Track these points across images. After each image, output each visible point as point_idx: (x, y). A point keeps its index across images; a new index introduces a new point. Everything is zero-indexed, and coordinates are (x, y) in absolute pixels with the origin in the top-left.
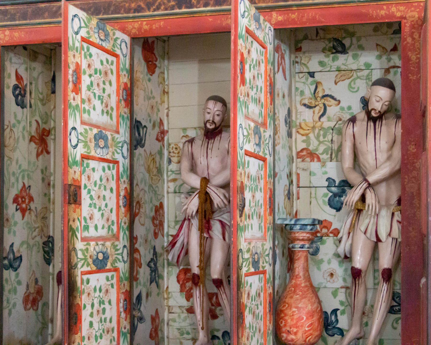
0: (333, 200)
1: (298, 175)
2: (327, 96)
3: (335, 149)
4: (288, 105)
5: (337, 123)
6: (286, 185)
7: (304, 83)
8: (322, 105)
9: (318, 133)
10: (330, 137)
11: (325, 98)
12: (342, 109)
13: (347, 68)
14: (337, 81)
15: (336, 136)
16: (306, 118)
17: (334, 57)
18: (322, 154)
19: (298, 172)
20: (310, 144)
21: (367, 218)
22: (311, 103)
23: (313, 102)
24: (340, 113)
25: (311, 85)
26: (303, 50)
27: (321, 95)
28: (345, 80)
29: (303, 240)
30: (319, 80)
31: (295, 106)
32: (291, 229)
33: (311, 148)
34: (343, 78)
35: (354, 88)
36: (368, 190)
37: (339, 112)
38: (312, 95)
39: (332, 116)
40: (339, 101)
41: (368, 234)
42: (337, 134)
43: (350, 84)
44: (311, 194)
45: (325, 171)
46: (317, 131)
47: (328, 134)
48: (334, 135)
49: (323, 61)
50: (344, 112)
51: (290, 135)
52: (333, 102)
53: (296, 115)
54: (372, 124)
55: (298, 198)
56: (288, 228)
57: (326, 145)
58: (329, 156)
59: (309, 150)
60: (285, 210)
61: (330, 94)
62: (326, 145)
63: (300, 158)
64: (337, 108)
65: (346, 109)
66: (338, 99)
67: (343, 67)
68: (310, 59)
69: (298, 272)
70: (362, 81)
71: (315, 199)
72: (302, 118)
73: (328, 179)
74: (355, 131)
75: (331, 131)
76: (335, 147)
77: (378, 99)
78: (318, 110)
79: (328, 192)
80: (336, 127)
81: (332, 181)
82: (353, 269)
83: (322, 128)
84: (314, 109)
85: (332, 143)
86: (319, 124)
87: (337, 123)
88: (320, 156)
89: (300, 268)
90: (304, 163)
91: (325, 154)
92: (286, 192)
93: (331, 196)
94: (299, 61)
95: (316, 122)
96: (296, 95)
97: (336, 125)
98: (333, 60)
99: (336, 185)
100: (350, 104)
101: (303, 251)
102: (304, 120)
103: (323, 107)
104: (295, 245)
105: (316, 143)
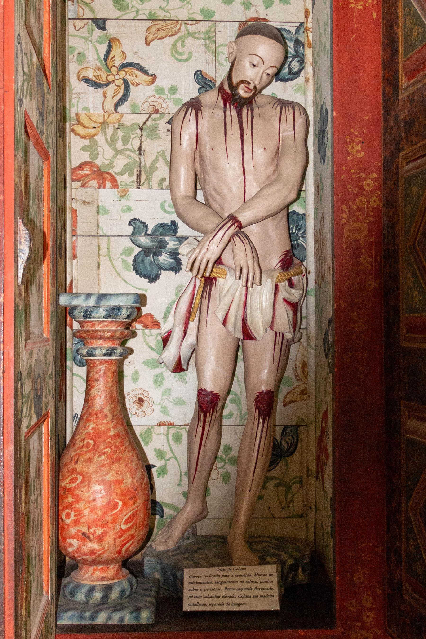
0: (143, 261)
1: (74, 212)
2: (131, 65)
3: (145, 165)
5: (150, 116)
8: (120, 83)
10: (136, 144)
12: (160, 91)
13: (168, 15)
14: (150, 38)
16: (90, 106)
18: (121, 174)
19: (74, 206)
20: (98, 154)
22: (99, 77)
23: (104, 76)
24: (155, 99)
25: (100, 43)
27: (118, 62)
28: (165, 37)
30: (115, 36)
33: (99, 162)
34: (161, 34)
37: (154, 96)
38: (100, 61)
39: (140, 104)
40: (154, 77)
43: (174, 45)
44: (99, 248)
45: (127, 206)
46: (110, 131)
47: (133, 136)
48: (144, 138)
50: (163, 96)
52: (142, 77)
54: (234, 113)
55: (74, 257)
57: (128, 157)
58: (134, 178)
59: (96, 165)
62: (128, 157)
63: (78, 180)
64: (150, 90)
65: (167, 92)
66: (151, 72)
67: (161, 14)
71: (107, 258)
72: (82, 105)
73: (133, 222)
75: (139, 131)
77: (256, 60)
79: (133, 246)
80: (148, 123)
81: (141, 225)
83: (120, 126)
84: (105, 89)
85: (140, 154)
86: (115, 117)
87: (150, 116)
88: (116, 177)
90: (85, 190)
93: (138, 254)
97: (147, 120)
99: (149, 232)
102: (85, 108)
105: (109, 152)
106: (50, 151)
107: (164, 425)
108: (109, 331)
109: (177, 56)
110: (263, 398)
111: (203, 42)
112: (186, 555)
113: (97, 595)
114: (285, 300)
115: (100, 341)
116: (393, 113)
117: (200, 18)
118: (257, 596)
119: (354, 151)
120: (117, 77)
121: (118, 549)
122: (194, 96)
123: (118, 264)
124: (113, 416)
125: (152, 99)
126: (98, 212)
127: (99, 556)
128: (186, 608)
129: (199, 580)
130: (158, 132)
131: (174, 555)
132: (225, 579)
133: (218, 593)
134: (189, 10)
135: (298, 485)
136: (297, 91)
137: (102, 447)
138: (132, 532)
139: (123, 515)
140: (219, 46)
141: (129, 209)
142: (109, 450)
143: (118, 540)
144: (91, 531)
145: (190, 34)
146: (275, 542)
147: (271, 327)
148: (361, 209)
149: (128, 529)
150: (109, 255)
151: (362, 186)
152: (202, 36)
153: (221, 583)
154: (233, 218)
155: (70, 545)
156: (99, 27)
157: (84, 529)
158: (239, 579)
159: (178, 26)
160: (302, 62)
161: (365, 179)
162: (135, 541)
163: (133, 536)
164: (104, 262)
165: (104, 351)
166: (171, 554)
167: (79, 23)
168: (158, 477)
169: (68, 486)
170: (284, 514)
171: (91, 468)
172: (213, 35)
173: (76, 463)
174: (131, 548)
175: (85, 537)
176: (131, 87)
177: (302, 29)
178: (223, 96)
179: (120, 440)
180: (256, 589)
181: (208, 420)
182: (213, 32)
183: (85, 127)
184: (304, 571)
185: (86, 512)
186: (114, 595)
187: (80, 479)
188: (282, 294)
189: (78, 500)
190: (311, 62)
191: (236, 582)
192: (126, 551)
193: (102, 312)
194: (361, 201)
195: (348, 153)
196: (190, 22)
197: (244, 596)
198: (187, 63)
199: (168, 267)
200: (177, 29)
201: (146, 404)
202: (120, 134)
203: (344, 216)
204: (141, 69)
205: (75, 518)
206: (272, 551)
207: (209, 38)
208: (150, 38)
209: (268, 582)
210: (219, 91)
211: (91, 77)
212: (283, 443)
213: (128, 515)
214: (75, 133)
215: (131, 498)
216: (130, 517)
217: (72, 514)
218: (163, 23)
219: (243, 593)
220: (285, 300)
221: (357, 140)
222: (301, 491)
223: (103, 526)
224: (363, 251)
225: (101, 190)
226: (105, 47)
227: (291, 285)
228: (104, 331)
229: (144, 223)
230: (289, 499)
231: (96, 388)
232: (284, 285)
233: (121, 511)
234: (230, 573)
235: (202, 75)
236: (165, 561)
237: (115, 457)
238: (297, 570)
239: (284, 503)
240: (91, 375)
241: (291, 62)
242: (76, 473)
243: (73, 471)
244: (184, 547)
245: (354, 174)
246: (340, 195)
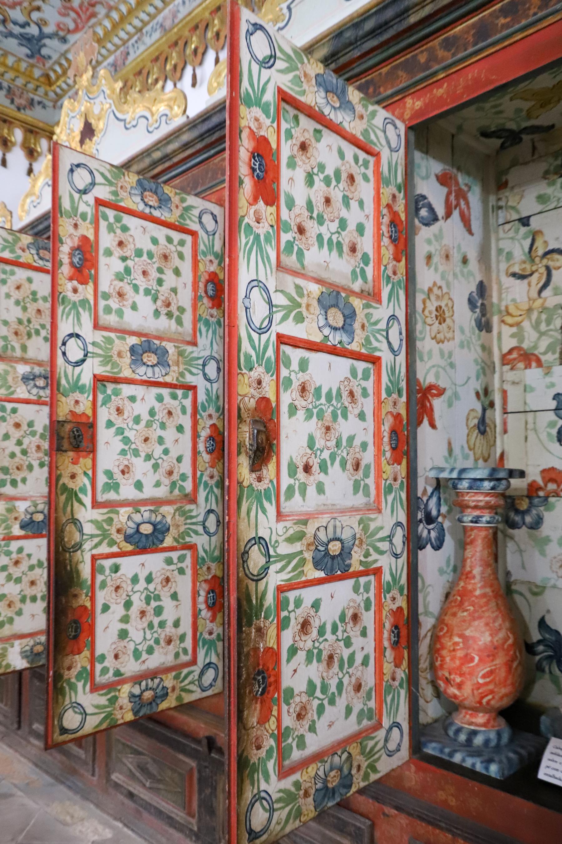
1: (504, 393)
7: (512, 238)
8: (543, 270)
18: (545, 353)
22: (524, 270)
23: (528, 266)
25: (525, 238)
26: (510, 185)
33: (525, 346)
44: (526, 423)
46: (535, 316)
53: (500, 293)
55: (505, 431)
57: (551, 336)
60: (471, 453)
62: (551, 336)
63: (507, 364)
68: (522, 197)
71: (533, 432)
78: (536, 280)
83: (544, 309)
86: (539, 302)
90: (514, 372)
91: (550, 353)
95: (534, 301)
102: (514, 300)
123: (543, 436)
124: (482, 577)
137: (466, 604)
142: (472, 608)
150: (535, 430)
162: (497, 697)
163: (492, 692)
164: (532, 436)
167: (507, 227)
179: (485, 600)
213: (485, 671)
216: (487, 672)
225: (528, 371)
226: (529, 241)
237: (476, 615)
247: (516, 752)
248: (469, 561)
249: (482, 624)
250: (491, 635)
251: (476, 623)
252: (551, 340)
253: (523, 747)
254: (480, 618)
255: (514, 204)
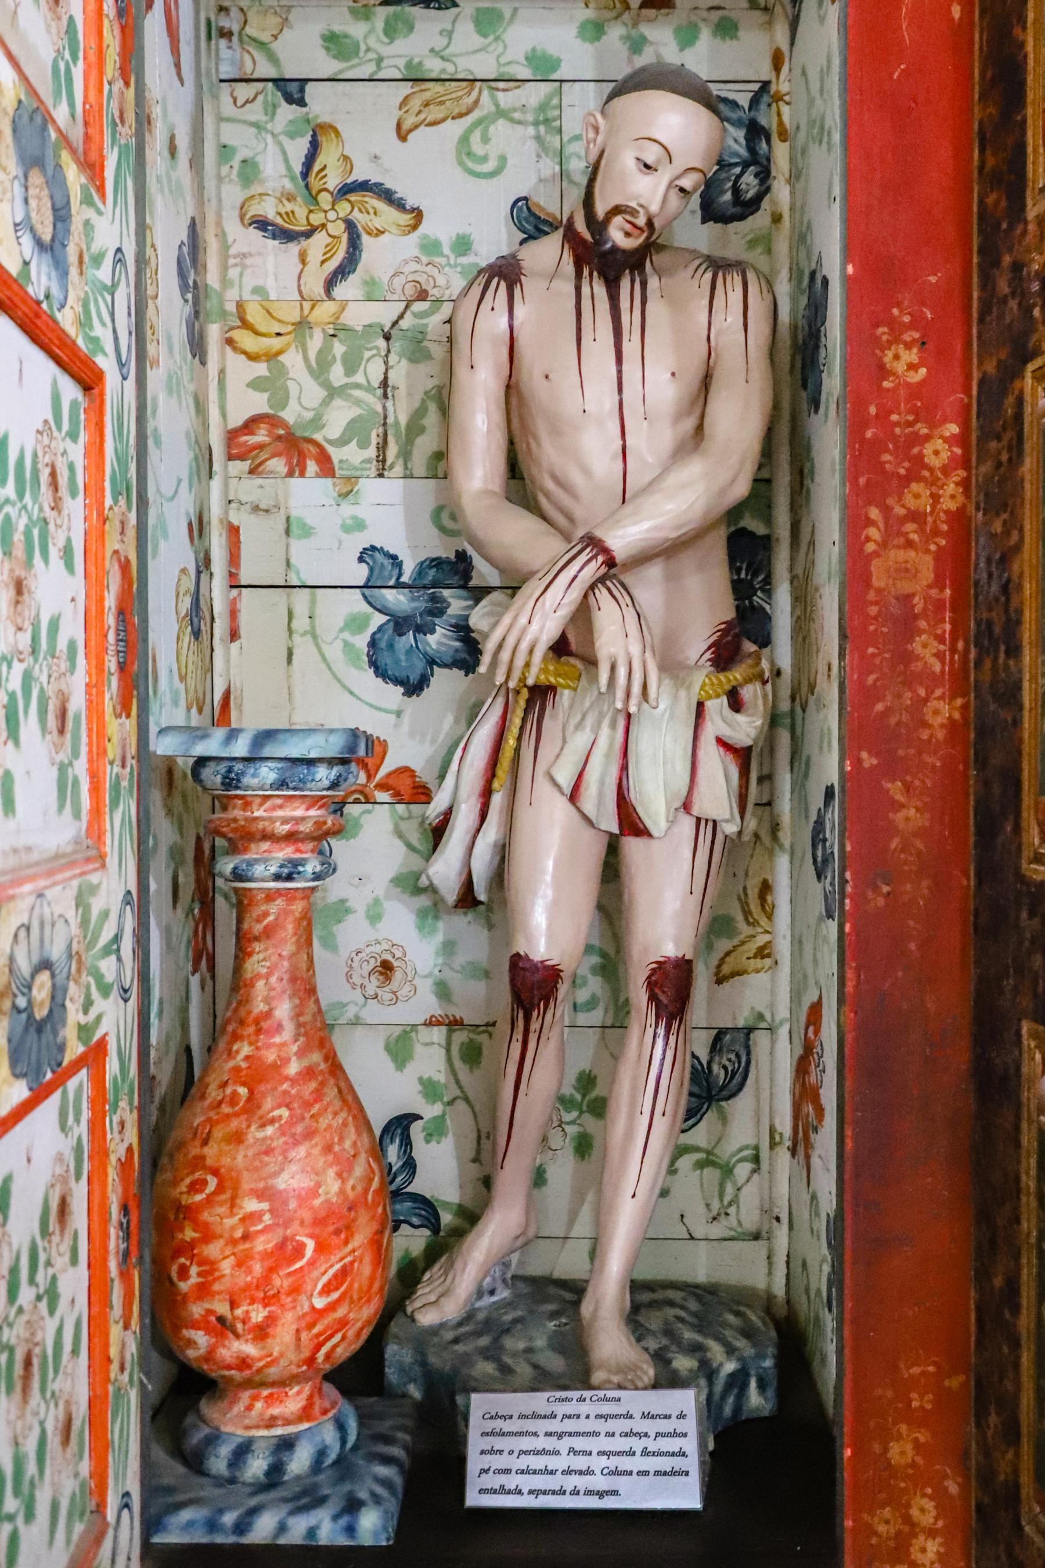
0: (391, 646)
1: (233, 531)
2: (363, 186)
3: (397, 423)
4: (191, 212)
5: (407, 307)
6: (184, 571)
7: (256, 125)
8: (338, 229)
9: (320, 352)
10: (375, 371)
11: (353, 197)
12: (431, 247)
13: (450, 68)
14: (409, 122)
15: (404, 362)
16: (271, 285)
17: (396, 17)
18: (342, 442)
19: (234, 519)
20: (287, 397)
21: (579, 726)
22: (290, 215)
23: (301, 212)
24: (418, 267)
25: (292, 136)
27: (333, 181)
29: (291, 837)
31: (219, 223)
32: (230, 781)
33: (289, 415)
34: (435, 112)
35: (485, 159)
36: (602, 594)
37: (417, 260)
38: (293, 178)
39: (385, 279)
40: (418, 214)
41: (589, 802)
42: (412, 360)
43: (464, 139)
45: (355, 518)
46: (315, 342)
47: (367, 354)
48: (393, 359)
49: (346, 36)
51: (197, 347)
52: (388, 215)
53: (224, 268)
54: (601, 290)
55: (234, 635)
56: (212, 776)
57: (358, 402)
58: (372, 452)
59: (283, 423)
60: (182, 687)
61: (374, 179)
62: (358, 402)
63: (241, 457)
65: (446, 250)
66: (410, 203)
67: (434, 66)
69: (267, 1000)
70: (520, 128)
71: (308, 638)
72: (249, 282)
74: (516, 323)
75: (382, 343)
76: (401, 412)
80: (404, 324)
81: (387, 562)
82: (518, 964)
83: (338, 331)
84: (304, 243)
87: (407, 307)
88: (330, 449)
89: (273, 980)
92: (186, 603)
93: (380, 629)
94: (235, 28)
96: (220, 179)
97: (401, 317)
98: (390, 32)
99: (405, 579)
100: (468, 230)
101: (289, 895)
102: (258, 290)
103: (345, 238)
104: (250, 863)
105: (314, 394)
106: (106, 363)
107: (439, 1023)
108: (285, 821)
109: (470, 164)
110: (666, 975)
111: (531, 130)
112: (484, 1341)
113: (257, 1466)
114: (720, 741)
115: (265, 846)
116: (1007, 260)
117: (525, 73)
118: (645, 1473)
119: (900, 367)
120: (332, 215)
121: (306, 1353)
122: (505, 251)
123: (335, 652)
124: (299, 1025)
125: (414, 266)
126: (287, 532)
127: (259, 1371)
128: (473, 1499)
129: (507, 1426)
130: (425, 343)
131: (456, 1341)
132: (570, 1426)
133: (552, 1462)
134: (498, 57)
135: (748, 1166)
136: (752, 244)
137: (268, 1103)
138: (341, 1312)
139: (316, 1274)
140: (570, 141)
141: (359, 525)
142: (284, 1112)
143: (304, 1336)
144: (239, 1312)
145: (501, 113)
146: (693, 1305)
147: (687, 806)
148: (915, 516)
149: (331, 1307)
151: (921, 457)
152: (530, 118)
153: (560, 1436)
154: (593, 542)
155: (191, 1343)
156: (290, 99)
157: (222, 1308)
158: (601, 1426)
159: (475, 94)
160: (765, 175)
161: (928, 438)
162: (351, 1333)
163: (343, 1323)
164: (303, 647)
165: (273, 869)
166: (450, 1335)
167: (244, 91)
168: (428, 1142)
169: (186, 1200)
170: (716, 1230)
171: (240, 1158)
172: (557, 113)
173: (205, 1142)
174: (339, 1350)
175: (223, 1327)
176: (365, 239)
177: (766, 99)
178: (574, 249)
179: (313, 1085)
180: (645, 1453)
181: (535, 1026)
182: (554, 108)
183: (257, 333)
184: (762, 1386)
185: (226, 1266)
186: (299, 1462)
187: (212, 1183)
188: (714, 725)
189: (208, 1236)
190: (787, 175)
191: (596, 1434)
192: (328, 1356)
193: (267, 773)
194: (917, 496)
195: (883, 371)
196: (501, 85)
197: (616, 1473)
198: (494, 180)
199: (448, 660)
200: (470, 100)
201: (398, 975)
202: (339, 348)
203: (873, 532)
204: (388, 196)
205: (201, 1280)
206: (689, 1335)
207: (546, 121)
208: (409, 122)
209: (675, 1434)
210: (565, 236)
211: (271, 215)
212: (715, 1068)
213: (331, 1272)
214: (235, 349)
215: (337, 1232)
216: (335, 1276)
217: (194, 1270)
218: (437, 88)
219: (614, 1462)
220: (720, 741)
221: (907, 337)
222: (756, 1176)
223: (266, 1302)
224: (923, 624)
225: (296, 482)
227: (736, 703)
228: (272, 820)
229: (394, 557)
230: (727, 1199)
231: (255, 958)
232: (716, 707)
233: (312, 1263)
234: (584, 1409)
235: (529, 209)
236: (433, 1360)
237: (299, 1129)
238: (744, 1387)
239: (716, 1205)
240: (246, 926)
241: (739, 177)
242: (204, 1167)
243: (199, 1162)
244: (481, 1316)
245: (898, 424)
246: (862, 481)
247: (387, 1460)
248: (260, 984)
249: (316, 1151)
250: (339, 1175)
251: (301, 1151)
252: (356, 412)
253: (388, 1440)
254: (309, 1135)
255: (265, 37)
